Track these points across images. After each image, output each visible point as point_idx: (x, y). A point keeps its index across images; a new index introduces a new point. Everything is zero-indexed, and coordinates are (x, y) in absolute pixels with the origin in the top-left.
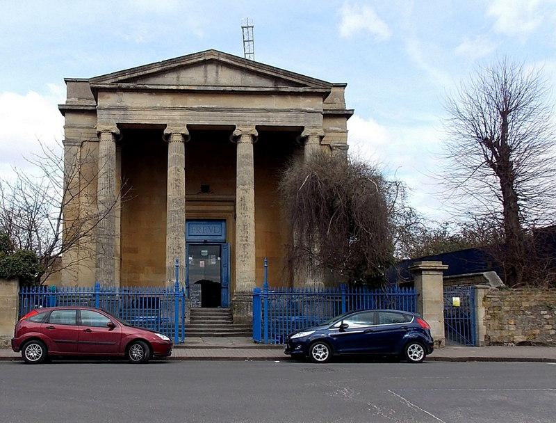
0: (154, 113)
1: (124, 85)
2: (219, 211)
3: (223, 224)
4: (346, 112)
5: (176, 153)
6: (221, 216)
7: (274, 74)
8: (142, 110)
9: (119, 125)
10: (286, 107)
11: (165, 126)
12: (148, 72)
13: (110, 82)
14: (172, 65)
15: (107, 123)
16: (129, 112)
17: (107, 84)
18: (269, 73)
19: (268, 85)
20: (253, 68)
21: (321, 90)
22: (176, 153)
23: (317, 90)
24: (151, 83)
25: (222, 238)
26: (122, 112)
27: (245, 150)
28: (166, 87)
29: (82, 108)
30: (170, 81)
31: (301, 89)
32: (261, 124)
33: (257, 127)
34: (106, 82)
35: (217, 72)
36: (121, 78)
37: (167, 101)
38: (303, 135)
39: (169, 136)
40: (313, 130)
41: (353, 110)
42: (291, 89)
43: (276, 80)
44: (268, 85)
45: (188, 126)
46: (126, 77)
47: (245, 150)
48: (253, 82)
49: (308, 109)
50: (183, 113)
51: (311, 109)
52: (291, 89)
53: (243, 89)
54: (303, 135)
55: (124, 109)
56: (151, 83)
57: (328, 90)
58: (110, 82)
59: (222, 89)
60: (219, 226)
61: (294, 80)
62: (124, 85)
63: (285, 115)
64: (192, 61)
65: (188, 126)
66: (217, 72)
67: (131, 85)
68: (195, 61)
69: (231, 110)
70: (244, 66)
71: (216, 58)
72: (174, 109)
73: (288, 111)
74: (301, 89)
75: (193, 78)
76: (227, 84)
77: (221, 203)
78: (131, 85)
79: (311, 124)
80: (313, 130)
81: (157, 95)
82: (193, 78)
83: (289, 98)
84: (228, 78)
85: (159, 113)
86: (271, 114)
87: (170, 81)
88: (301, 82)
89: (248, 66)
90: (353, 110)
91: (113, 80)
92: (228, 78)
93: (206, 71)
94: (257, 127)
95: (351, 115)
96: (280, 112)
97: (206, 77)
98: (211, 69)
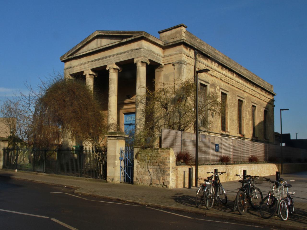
7: (119, 34)
13: (65, 57)
16: (73, 68)
19: (116, 41)
20: (111, 34)
21: (138, 37)
31: (130, 39)
34: (65, 58)
37: (84, 60)
43: (123, 37)
44: (116, 41)
52: (125, 40)
56: (77, 54)
58: (65, 57)
62: (70, 57)
63: (125, 54)
69: (105, 58)
72: (86, 63)
73: (127, 52)
74: (130, 39)
75: (94, 45)
78: (72, 57)
79: (137, 56)
80: (138, 59)
82: (94, 45)
84: (105, 42)
86: (120, 55)
96: (123, 53)
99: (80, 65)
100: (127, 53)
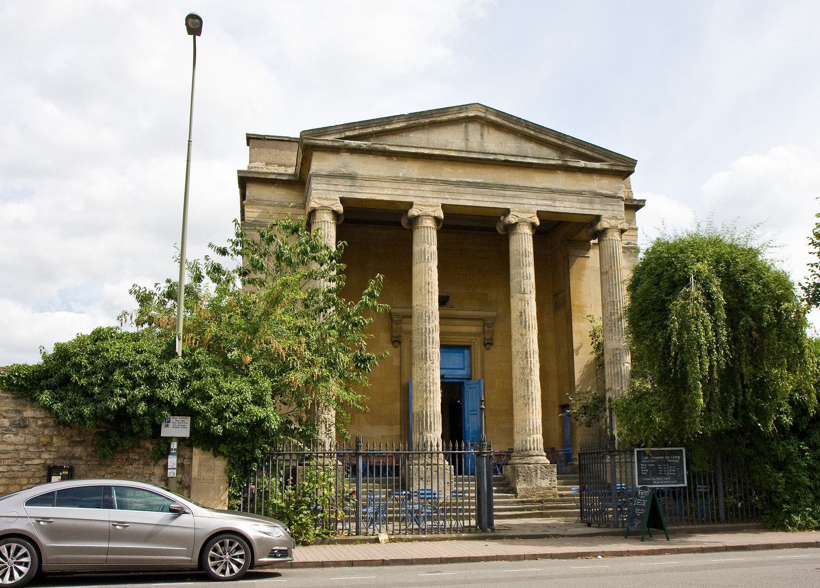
0: (395, 185)
1: (354, 143)
2: (460, 334)
3: (466, 352)
4: (636, 203)
5: (427, 245)
6: (464, 341)
7: (559, 142)
8: (378, 182)
9: (343, 200)
10: (575, 188)
11: (411, 205)
12: (387, 127)
13: (332, 138)
14: (423, 121)
15: (326, 197)
16: (358, 183)
17: (328, 140)
18: (553, 140)
19: (553, 158)
21: (621, 168)
22: (427, 245)
23: (617, 168)
24: (392, 143)
25: (464, 373)
26: (349, 182)
27: (523, 244)
28: (414, 150)
29: (273, 177)
30: (417, 141)
31: (597, 165)
32: (544, 209)
33: (539, 214)
35: (482, 135)
36: (348, 134)
37: (412, 169)
38: (599, 227)
39: (416, 219)
40: (613, 223)
41: (644, 201)
42: (582, 164)
44: (550, 157)
45: (444, 207)
46: (356, 133)
47: (523, 244)
48: (532, 152)
49: (604, 192)
50: (436, 188)
51: (609, 193)
52: (582, 164)
53: (519, 159)
54: (599, 227)
55: (352, 177)
56: (392, 143)
57: (630, 169)
58: (332, 138)
59: (492, 157)
60: (462, 354)
61: (587, 152)
62: (354, 143)
64: (450, 117)
65: (444, 207)
66: (482, 135)
67: (363, 144)
68: (454, 116)
70: (519, 128)
71: (482, 115)
72: (423, 181)
74: (597, 165)
75: (450, 140)
76: (497, 151)
77: (462, 322)
78: (363, 144)
79: (610, 213)
81: (398, 160)
82: (450, 140)
83: (580, 176)
84: (497, 144)
85: (402, 186)
87: (417, 141)
88: (596, 155)
89: (525, 130)
90: (644, 201)
91: (338, 136)
92: (497, 144)
93: (466, 133)
94: (539, 214)
95: (642, 206)
97: (467, 139)
98: (474, 130)
99: (395, 180)
100: (581, 198)
